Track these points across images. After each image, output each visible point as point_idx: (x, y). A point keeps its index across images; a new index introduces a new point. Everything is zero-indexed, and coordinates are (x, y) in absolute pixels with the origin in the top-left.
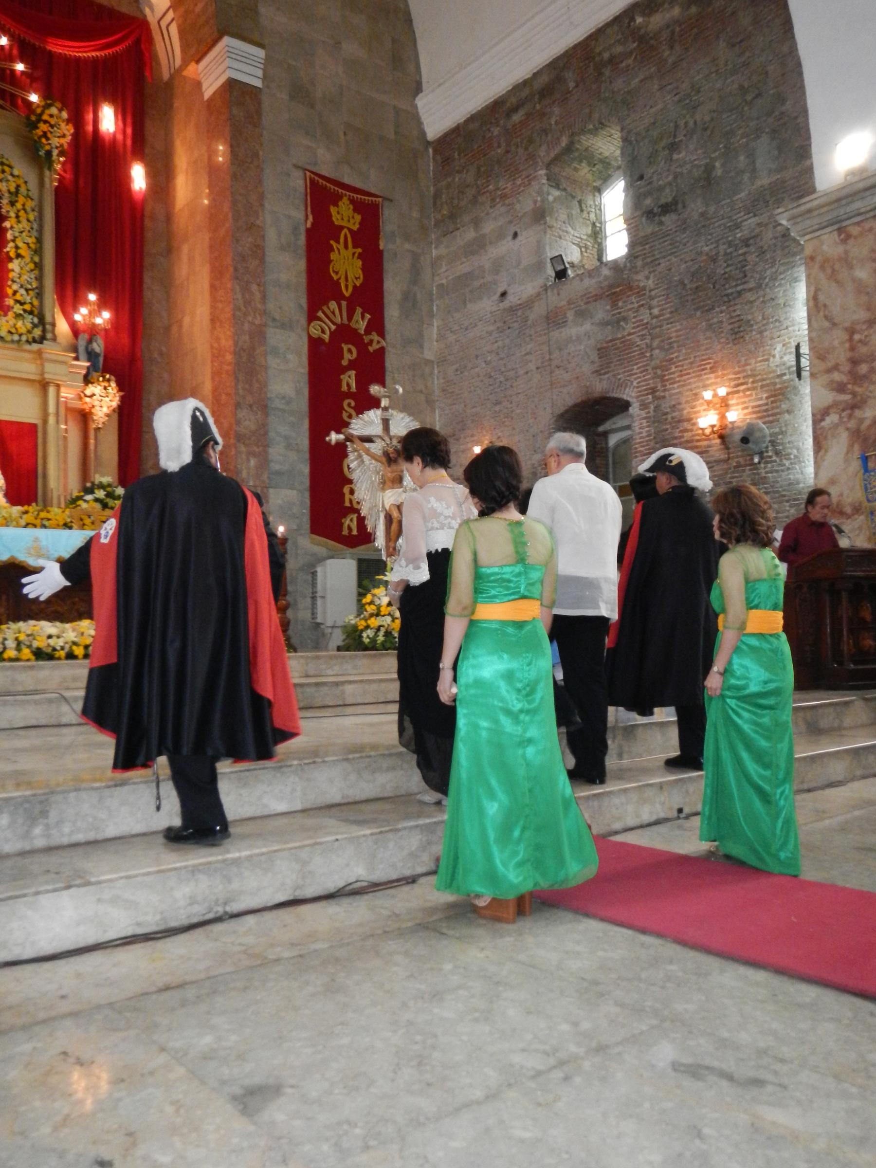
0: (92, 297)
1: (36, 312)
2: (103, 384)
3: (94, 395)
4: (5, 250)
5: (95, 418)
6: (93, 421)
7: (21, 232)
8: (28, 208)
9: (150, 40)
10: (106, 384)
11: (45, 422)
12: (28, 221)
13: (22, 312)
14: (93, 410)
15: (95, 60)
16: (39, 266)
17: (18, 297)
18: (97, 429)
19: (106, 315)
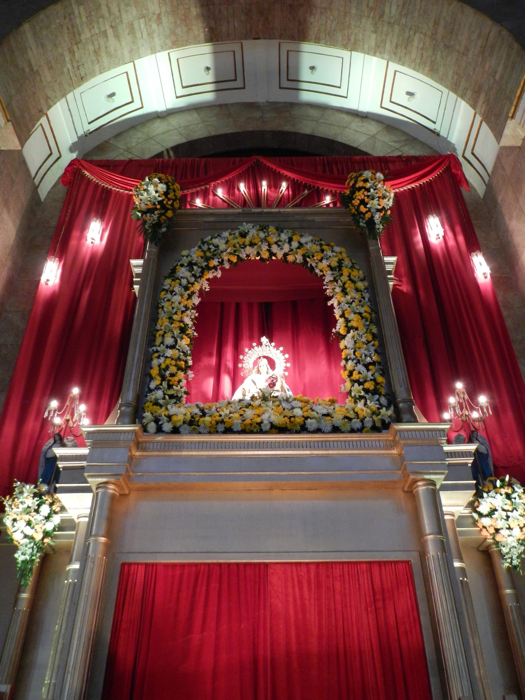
0: (459, 385)
1: (383, 391)
2: (503, 491)
3: (496, 510)
4: (334, 330)
5: (505, 550)
6: (502, 556)
7: (351, 303)
8: (356, 279)
9: (459, 165)
10: (510, 491)
11: (423, 555)
12: (357, 290)
13: (363, 393)
14: (498, 538)
15: (412, 191)
16: (378, 337)
17: (355, 376)
18: (512, 569)
19: (483, 399)
